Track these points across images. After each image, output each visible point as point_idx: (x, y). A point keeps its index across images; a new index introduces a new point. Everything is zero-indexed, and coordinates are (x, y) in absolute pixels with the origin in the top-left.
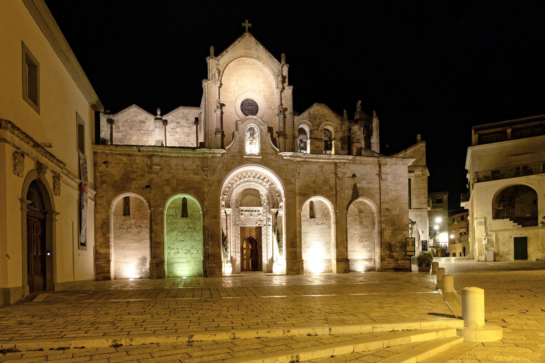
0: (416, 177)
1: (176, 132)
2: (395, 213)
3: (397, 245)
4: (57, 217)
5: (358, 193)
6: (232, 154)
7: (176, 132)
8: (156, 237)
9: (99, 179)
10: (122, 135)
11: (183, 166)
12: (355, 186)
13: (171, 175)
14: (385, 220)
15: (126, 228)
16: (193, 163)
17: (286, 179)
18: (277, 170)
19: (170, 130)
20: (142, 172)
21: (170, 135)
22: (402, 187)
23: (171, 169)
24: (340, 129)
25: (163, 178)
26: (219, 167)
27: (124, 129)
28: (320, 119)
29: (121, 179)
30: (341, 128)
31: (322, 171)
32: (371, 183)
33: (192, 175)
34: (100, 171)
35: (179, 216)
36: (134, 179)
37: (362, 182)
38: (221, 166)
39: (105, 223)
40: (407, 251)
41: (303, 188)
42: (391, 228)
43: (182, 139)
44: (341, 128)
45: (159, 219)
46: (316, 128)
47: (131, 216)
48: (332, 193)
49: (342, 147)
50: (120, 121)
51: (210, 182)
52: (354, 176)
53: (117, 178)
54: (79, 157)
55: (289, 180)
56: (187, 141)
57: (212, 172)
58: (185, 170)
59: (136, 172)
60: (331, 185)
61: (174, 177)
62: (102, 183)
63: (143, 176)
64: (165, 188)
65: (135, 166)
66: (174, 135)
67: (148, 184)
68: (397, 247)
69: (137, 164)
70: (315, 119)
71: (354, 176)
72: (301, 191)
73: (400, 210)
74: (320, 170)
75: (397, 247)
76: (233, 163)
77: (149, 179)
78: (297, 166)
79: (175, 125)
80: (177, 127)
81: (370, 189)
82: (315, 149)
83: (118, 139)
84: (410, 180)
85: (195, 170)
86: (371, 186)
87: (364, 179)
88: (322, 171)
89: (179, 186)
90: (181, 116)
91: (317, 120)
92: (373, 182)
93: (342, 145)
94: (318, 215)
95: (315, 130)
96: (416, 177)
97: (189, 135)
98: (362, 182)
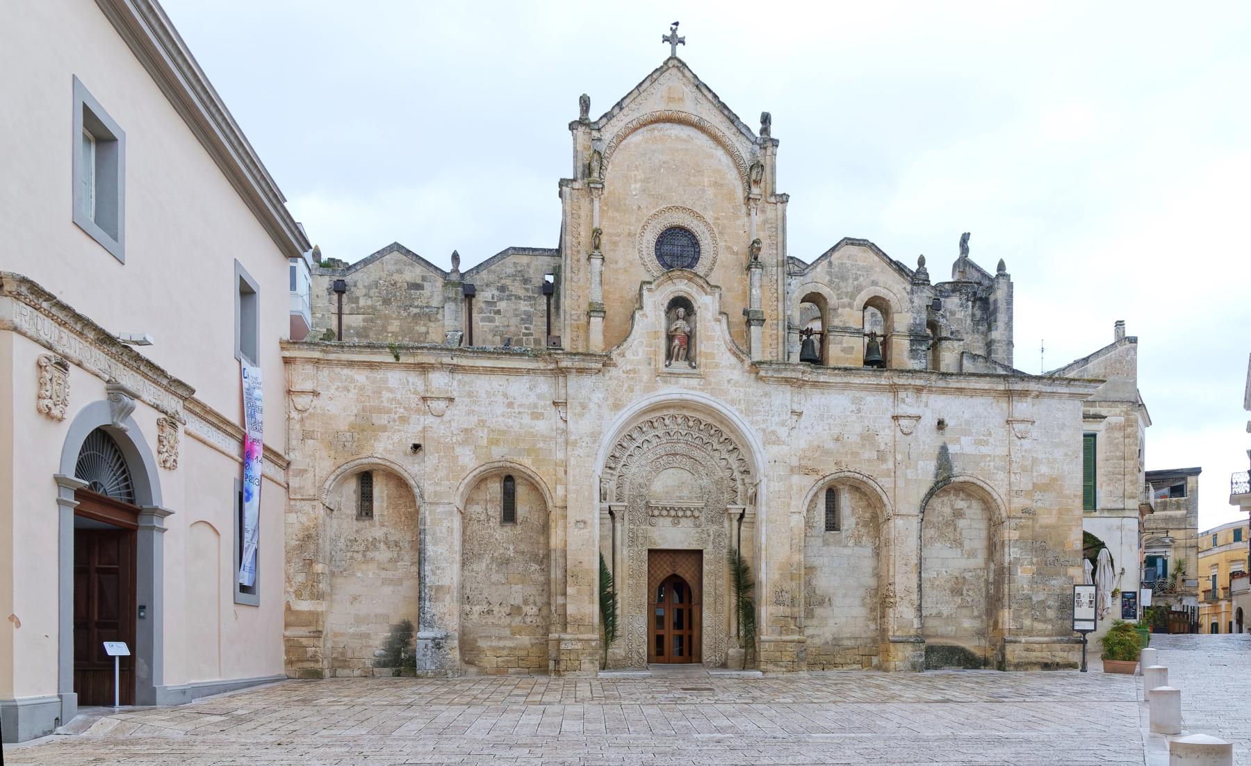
0: (1111, 428)
1: (498, 312)
2: (1045, 519)
3: (1050, 603)
4: (167, 522)
5: (951, 469)
6: (629, 367)
7: (498, 312)
8: (434, 574)
9: (298, 426)
10: (364, 320)
11: (505, 396)
12: (944, 449)
13: (474, 419)
15: (362, 548)
16: (531, 389)
17: (764, 431)
18: (743, 407)
19: (483, 306)
20: (402, 410)
21: (483, 319)
22: (1066, 455)
23: (475, 402)
25: (454, 425)
26: (596, 400)
27: (369, 302)
28: (856, 279)
29: (352, 427)
32: (986, 443)
33: (526, 420)
34: (299, 407)
35: (495, 522)
36: (384, 429)
38: (601, 396)
39: (309, 537)
40: (1074, 620)
41: (809, 454)
42: (1035, 560)
43: (513, 329)
44: (912, 302)
45: (444, 530)
46: (846, 300)
47: (376, 518)
48: (884, 467)
50: (360, 285)
51: (573, 438)
52: (941, 424)
53: (343, 425)
54: (242, 371)
55: (773, 432)
56: (525, 335)
57: (579, 410)
58: (510, 405)
59: (389, 411)
60: (882, 447)
61: (482, 423)
62: (306, 436)
63: (403, 420)
64: (458, 450)
65: (386, 395)
66: (491, 320)
67: (417, 442)
68: (1049, 607)
69: (390, 390)
70: (843, 278)
71: (941, 424)
72: (803, 462)
73: (1060, 513)
74: (854, 407)
75: (1049, 607)
76: (632, 391)
77: (420, 428)
78: (795, 399)
79: (496, 293)
80: (501, 299)
81: (984, 456)
82: (842, 354)
83: (354, 328)
84: (1090, 439)
85: (535, 406)
86: (985, 450)
87: (966, 433)
88: (859, 411)
89: (493, 447)
90: (510, 270)
91: (850, 281)
92: (991, 440)
93: (912, 345)
95: (844, 306)
96: (1111, 428)
97: (528, 318)
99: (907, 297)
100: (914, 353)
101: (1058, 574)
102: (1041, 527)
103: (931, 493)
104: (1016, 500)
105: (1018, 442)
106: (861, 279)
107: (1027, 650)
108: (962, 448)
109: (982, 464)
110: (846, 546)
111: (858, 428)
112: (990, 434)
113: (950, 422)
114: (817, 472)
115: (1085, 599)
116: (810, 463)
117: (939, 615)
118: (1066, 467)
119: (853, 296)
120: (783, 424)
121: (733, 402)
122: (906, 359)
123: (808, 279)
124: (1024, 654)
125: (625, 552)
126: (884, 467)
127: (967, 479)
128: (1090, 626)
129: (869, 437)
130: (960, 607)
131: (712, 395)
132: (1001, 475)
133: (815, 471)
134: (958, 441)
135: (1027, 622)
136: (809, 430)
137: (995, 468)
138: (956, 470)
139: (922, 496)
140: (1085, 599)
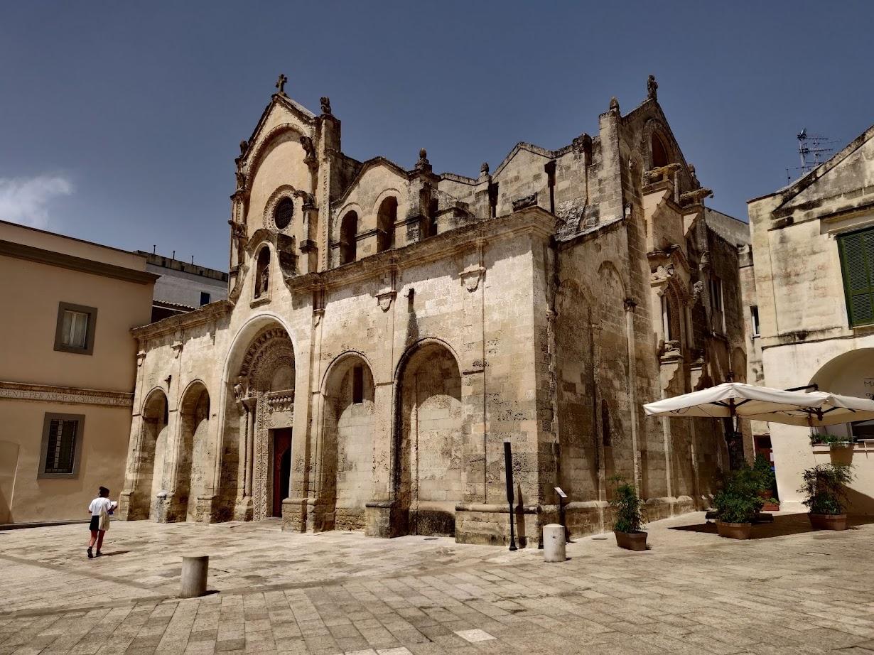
14: (473, 393)
17: (297, 330)
22: (516, 295)
24: (407, 195)
30: (409, 192)
37: (427, 302)
44: (409, 192)
48: (371, 342)
49: (408, 234)
60: (371, 326)
81: (443, 315)
86: (444, 309)
92: (450, 298)
93: (408, 228)
95: (366, 214)
98: (427, 302)
99: (406, 189)
100: (410, 235)
101: (512, 430)
102: (495, 379)
103: (404, 361)
104: (468, 353)
105: (470, 294)
107: (475, 519)
109: (441, 324)
111: (356, 314)
117: (433, 478)
118: (516, 309)
119: (372, 205)
120: (307, 323)
121: (283, 314)
123: (346, 203)
124: (472, 524)
126: (371, 342)
127: (429, 340)
129: (363, 319)
130: (450, 469)
131: (274, 311)
132: (457, 331)
134: (424, 305)
135: (480, 489)
136: (329, 323)
137: (452, 324)
138: (422, 334)
139: (396, 364)
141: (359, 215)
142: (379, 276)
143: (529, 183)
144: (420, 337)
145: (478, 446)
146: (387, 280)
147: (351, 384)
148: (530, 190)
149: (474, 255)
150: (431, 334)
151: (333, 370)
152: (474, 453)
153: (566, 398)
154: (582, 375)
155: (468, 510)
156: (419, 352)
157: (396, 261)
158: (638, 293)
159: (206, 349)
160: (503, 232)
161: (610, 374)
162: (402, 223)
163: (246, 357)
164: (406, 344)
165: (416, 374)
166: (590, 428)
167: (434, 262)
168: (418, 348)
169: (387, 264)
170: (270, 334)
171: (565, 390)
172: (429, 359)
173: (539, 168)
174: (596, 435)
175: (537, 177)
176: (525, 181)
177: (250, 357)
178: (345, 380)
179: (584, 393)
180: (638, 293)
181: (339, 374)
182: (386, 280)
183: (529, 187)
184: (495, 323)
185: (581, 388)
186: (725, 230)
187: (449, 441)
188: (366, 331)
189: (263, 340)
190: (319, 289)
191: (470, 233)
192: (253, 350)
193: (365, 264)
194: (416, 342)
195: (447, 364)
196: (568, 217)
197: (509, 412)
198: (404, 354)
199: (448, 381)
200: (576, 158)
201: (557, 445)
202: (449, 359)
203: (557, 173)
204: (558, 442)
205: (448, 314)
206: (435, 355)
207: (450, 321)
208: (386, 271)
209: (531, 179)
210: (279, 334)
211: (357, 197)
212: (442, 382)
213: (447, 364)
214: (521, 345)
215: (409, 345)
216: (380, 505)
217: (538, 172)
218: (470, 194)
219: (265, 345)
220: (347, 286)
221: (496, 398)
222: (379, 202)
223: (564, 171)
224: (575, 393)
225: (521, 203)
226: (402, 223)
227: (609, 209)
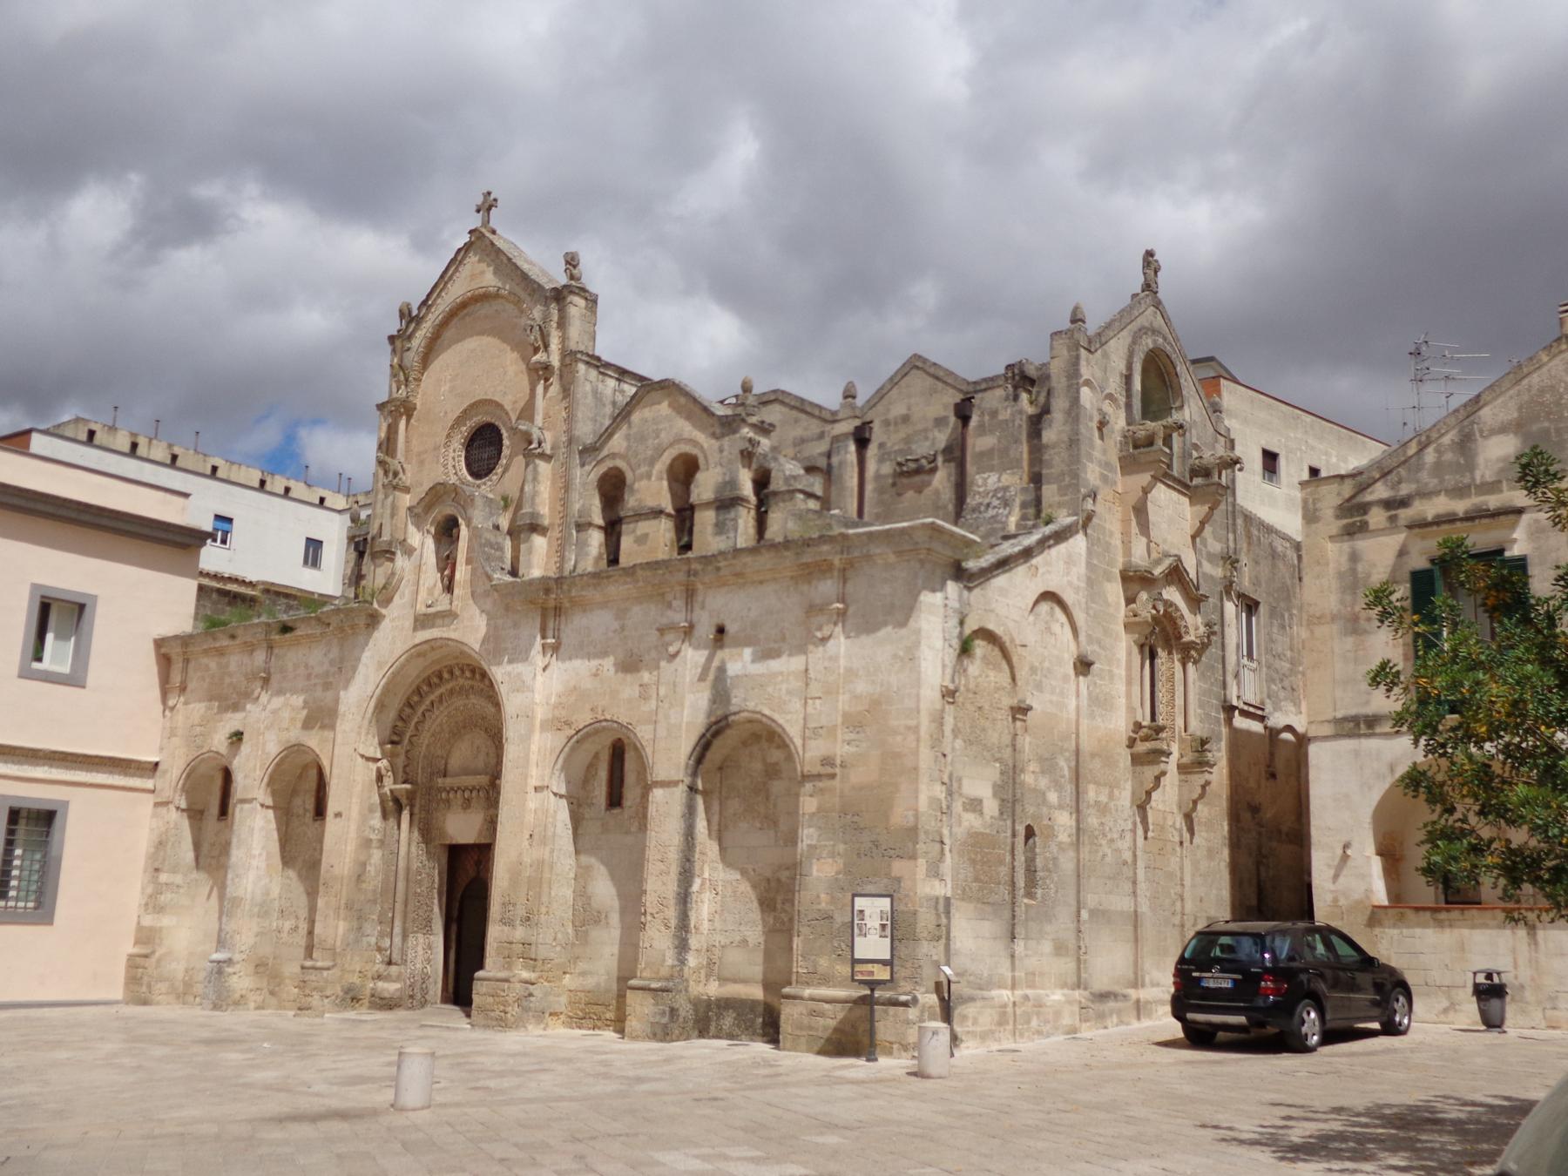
2: (858, 776)
11: (306, 666)
14: (819, 809)
22: (895, 656)
31: (623, 628)
33: (319, 693)
42: (841, 847)
46: (644, 469)
49: (717, 525)
52: (721, 630)
65: (227, 680)
72: (557, 713)
74: (616, 625)
78: (551, 625)
94: (631, 794)
95: (641, 477)
103: (704, 746)
106: (663, 435)
108: (744, 667)
109: (770, 689)
110: (628, 832)
112: (783, 639)
113: (731, 628)
114: (568, 724)
115: (873, 922)
116: (564, 713)
119: (652, 462)
122: (710, 538)
123: (605, 452)
125: (413, 849)
128: (882, 974)
133: (568, 724)
138: (736, 701)
140: (873, 922)
141: (629, 476)
142: (663, 595)
143: (926, 430)
144: (733, 709)
145: (823, 896)
146: (679, 603)
147: (603, 774)
148: (928, 443)
149: (829, 582)
150: (751, 705)
151: (573, 749)
152: (815, 907)
153: (965, 824)
154: (995, 786)
155: (801, 998)
156: (729, 732)
157: (696, 574)
158: (1099, 642)
159: (319, 688)
160: (878, 551)
161: (1043, 782)
162: (707, 505)
163: (401, 711)
164: (709, 716)
165: (720, 768)
166: (1004, 871)
167: (761, 582)
168: (728, 726)
169: (681, 576)
170: (451, 673)
171: (965, 810)
172: (745, 743)
173: (945, 407)
174: (1013, 884)
175: (940, 422)
176: (920, 427)
177: (408, 710)
178: (591, 767)
179: (996, 813)
180: (1099, 642)
181: (584, 757)
182: (675, 603)
183: (926, 438)
184: (856, 697)
185: (991, 807)
186: (1326, 453)
187: (773, 884)
188: (637, 689)
189: (435, 680)
190: (552, 604)
191: (825, 548)
192: (416, 698)
193: (639, 572)
194: (726, 717)
195: (776, 755)
196: (988, 505)
197: (876, 844)
198: (704, 735)
199: (776, 783)
200: (1007, 399)
201: (947, 900)
202: (778, 747)
203: (974, 421)
204: (949, 894)
205: (781, 673)
206: (756, 737)
207: (784, 687)
208: (678, 588)
209: (930, 424)
210: (468, 674)
211: (625, 444)
212: (765, 784)
213: (776, 755)
214: (899, 738)
215: (713, 719)
216: (654, 985)
217: (943, 413)
218: (821, 436)
219: (438, 692)
220: (604, 605)
221: (856, 819)
222: (667, 458)
223: (987, 418)
224: (981, 813)
225: (912, 465)
226: (707, 505)
227: (1057, 499)
